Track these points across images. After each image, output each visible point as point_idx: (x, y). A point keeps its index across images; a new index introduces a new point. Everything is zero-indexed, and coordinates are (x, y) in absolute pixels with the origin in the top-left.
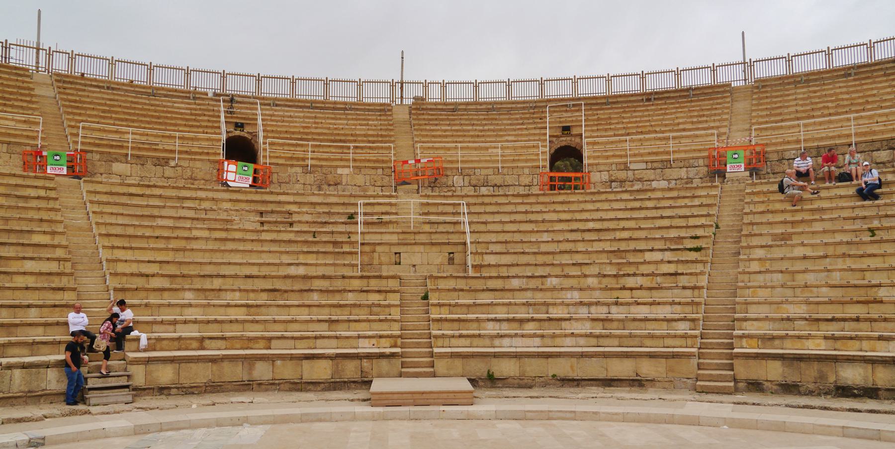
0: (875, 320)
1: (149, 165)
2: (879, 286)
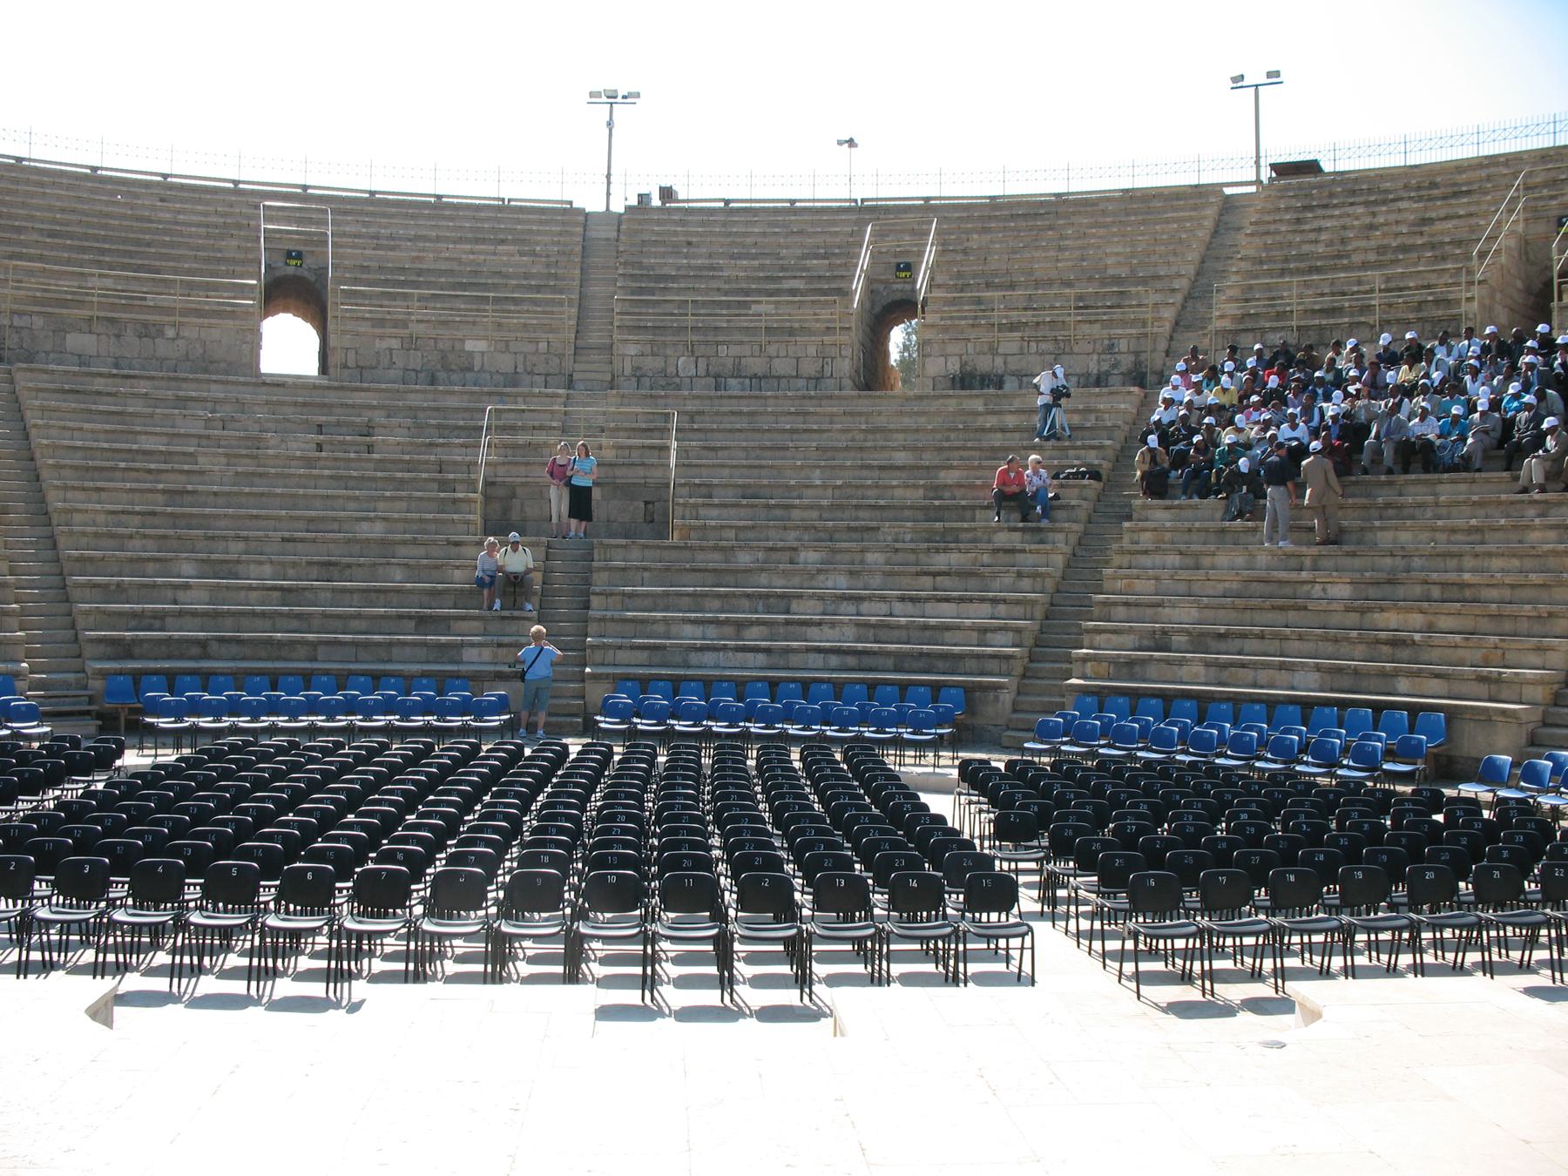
1: (130, 336)
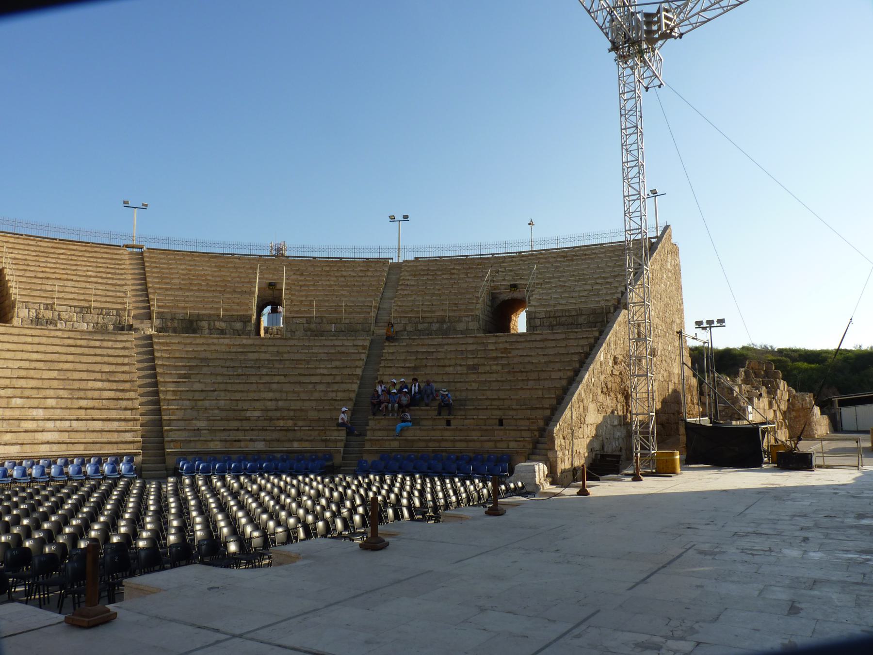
0: (247, 430)
2: (247, 410)
